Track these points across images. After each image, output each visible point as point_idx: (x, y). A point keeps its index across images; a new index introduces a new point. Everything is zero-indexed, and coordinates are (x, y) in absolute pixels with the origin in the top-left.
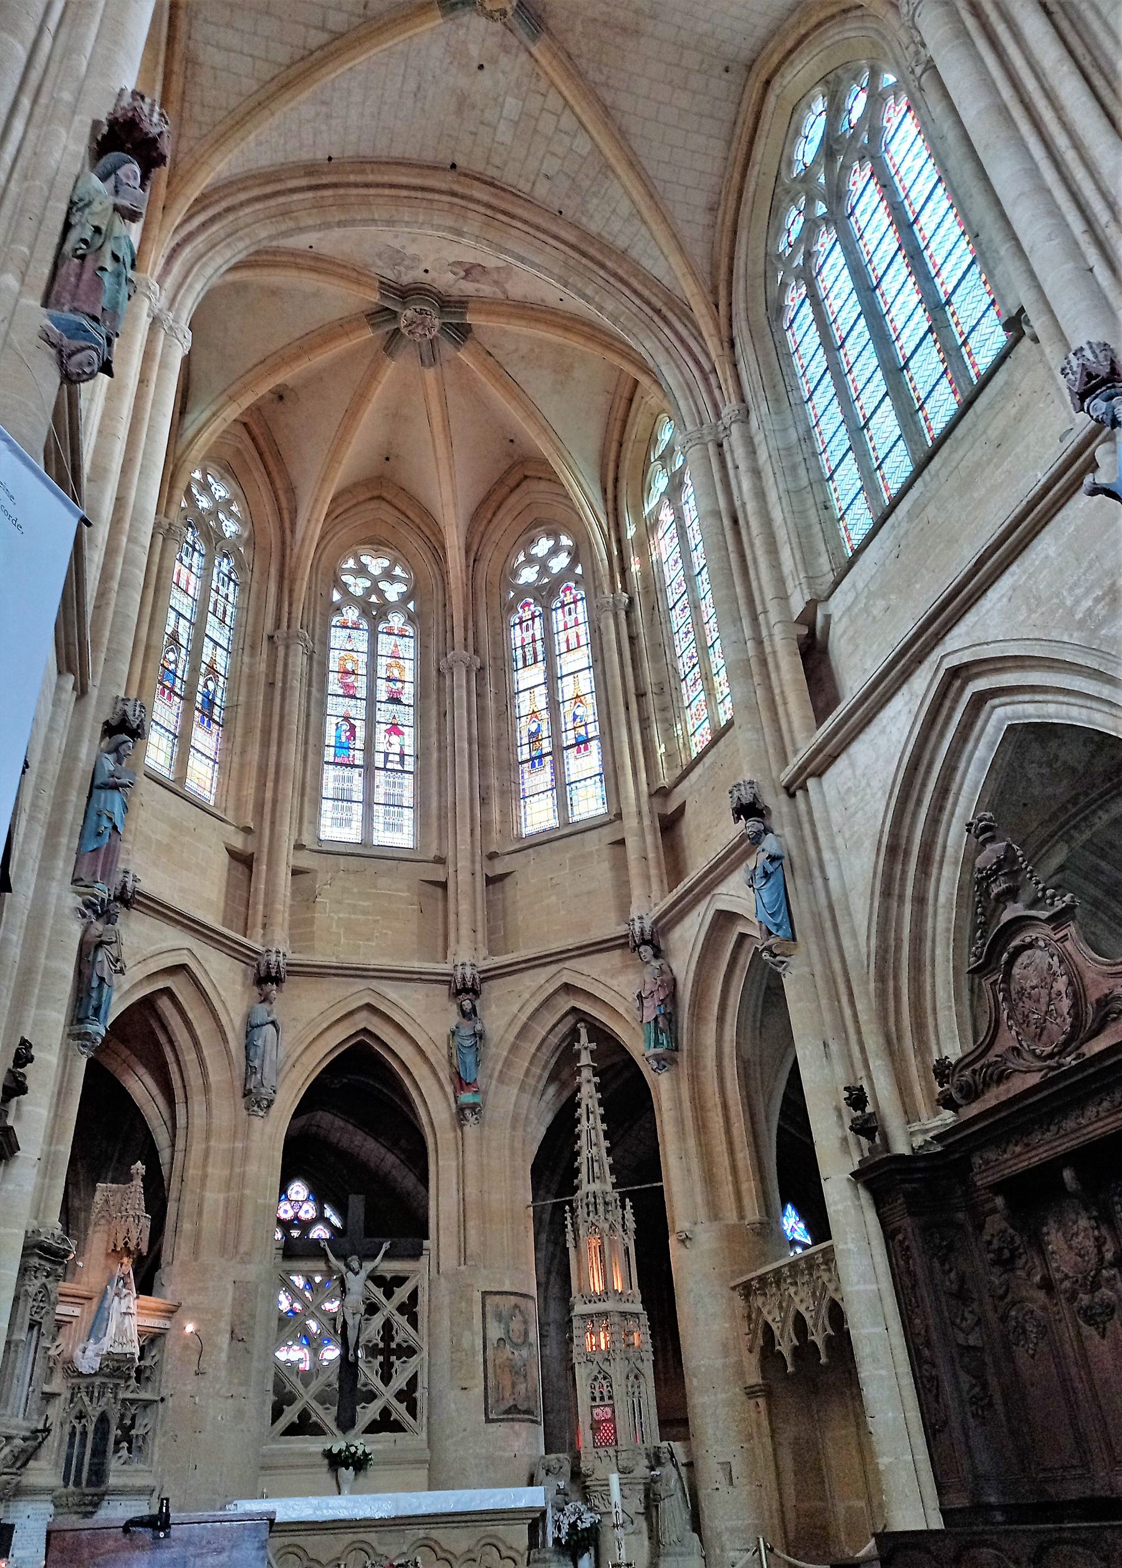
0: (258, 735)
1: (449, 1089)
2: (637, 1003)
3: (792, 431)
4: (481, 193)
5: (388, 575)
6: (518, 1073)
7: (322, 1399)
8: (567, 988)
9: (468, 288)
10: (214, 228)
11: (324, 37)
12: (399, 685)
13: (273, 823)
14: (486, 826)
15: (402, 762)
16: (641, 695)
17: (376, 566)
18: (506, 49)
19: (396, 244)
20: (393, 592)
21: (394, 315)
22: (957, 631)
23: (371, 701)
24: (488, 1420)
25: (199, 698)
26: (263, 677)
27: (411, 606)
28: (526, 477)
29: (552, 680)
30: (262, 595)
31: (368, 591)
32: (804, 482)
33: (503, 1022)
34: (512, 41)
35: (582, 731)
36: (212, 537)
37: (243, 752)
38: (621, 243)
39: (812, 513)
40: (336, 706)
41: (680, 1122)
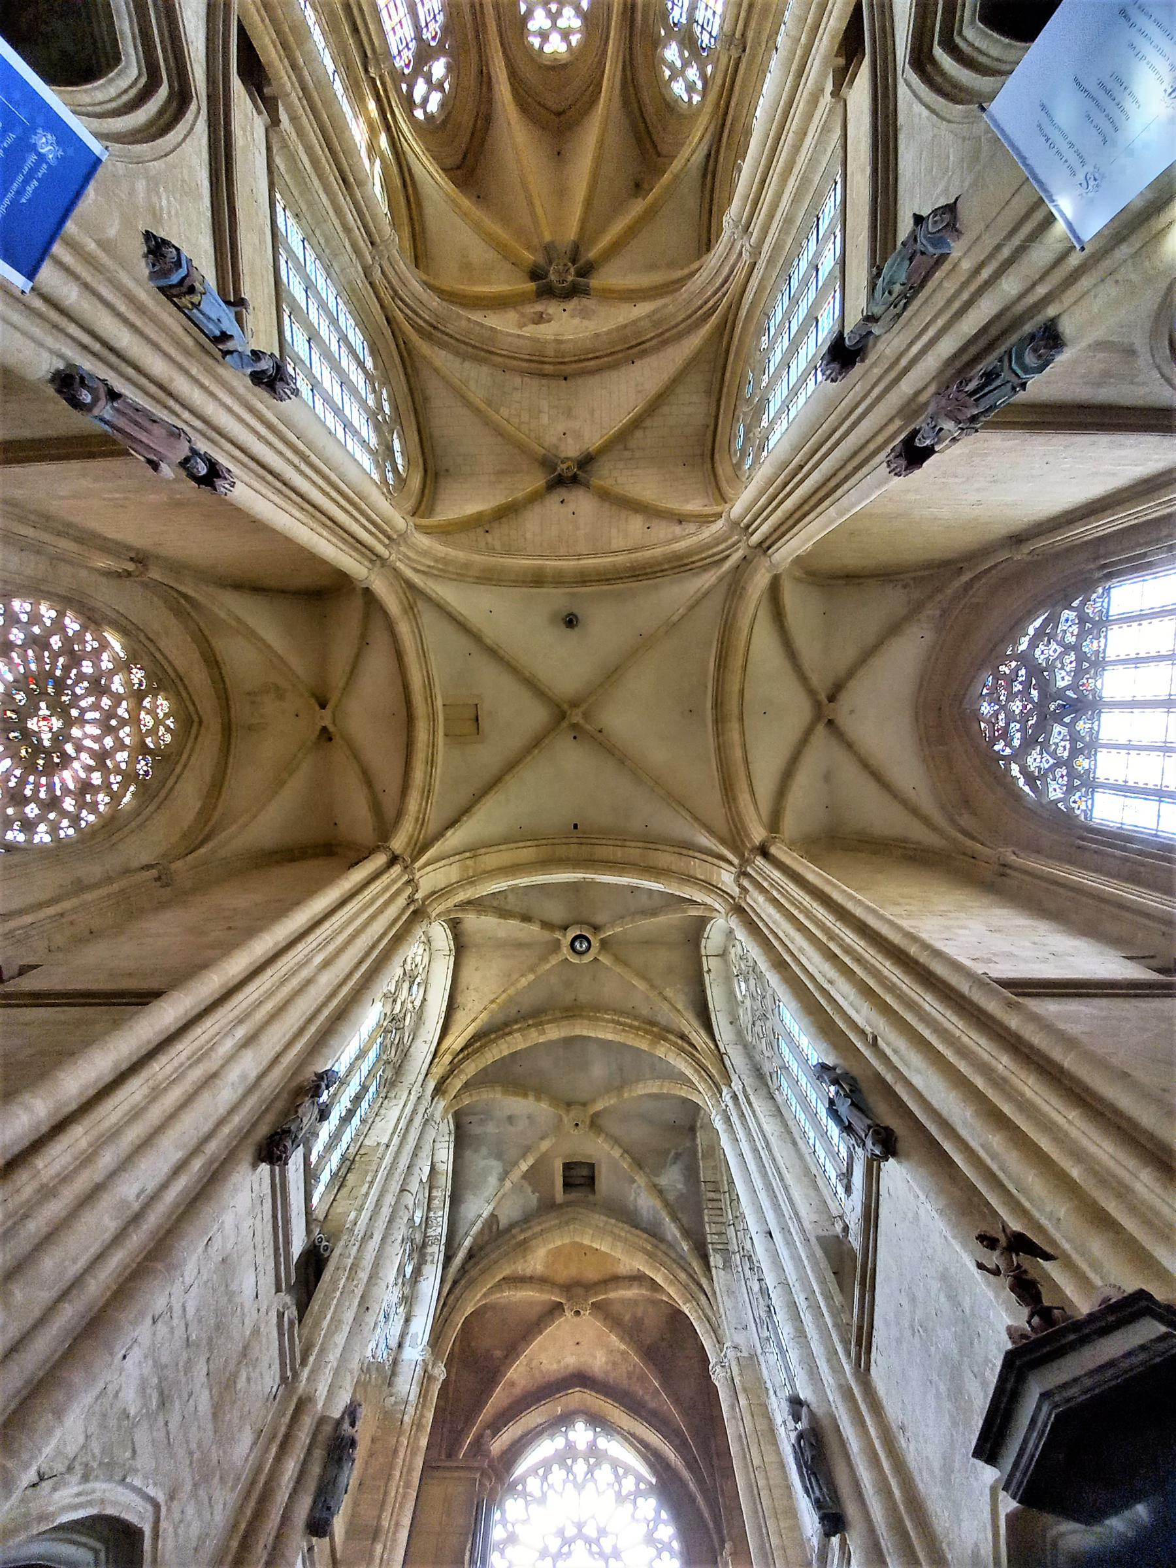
3: (338, 270)
10: (700, 303)
22: (205, 141)
32: (318, 232)
36: (688, 41)
39: (304, 208)
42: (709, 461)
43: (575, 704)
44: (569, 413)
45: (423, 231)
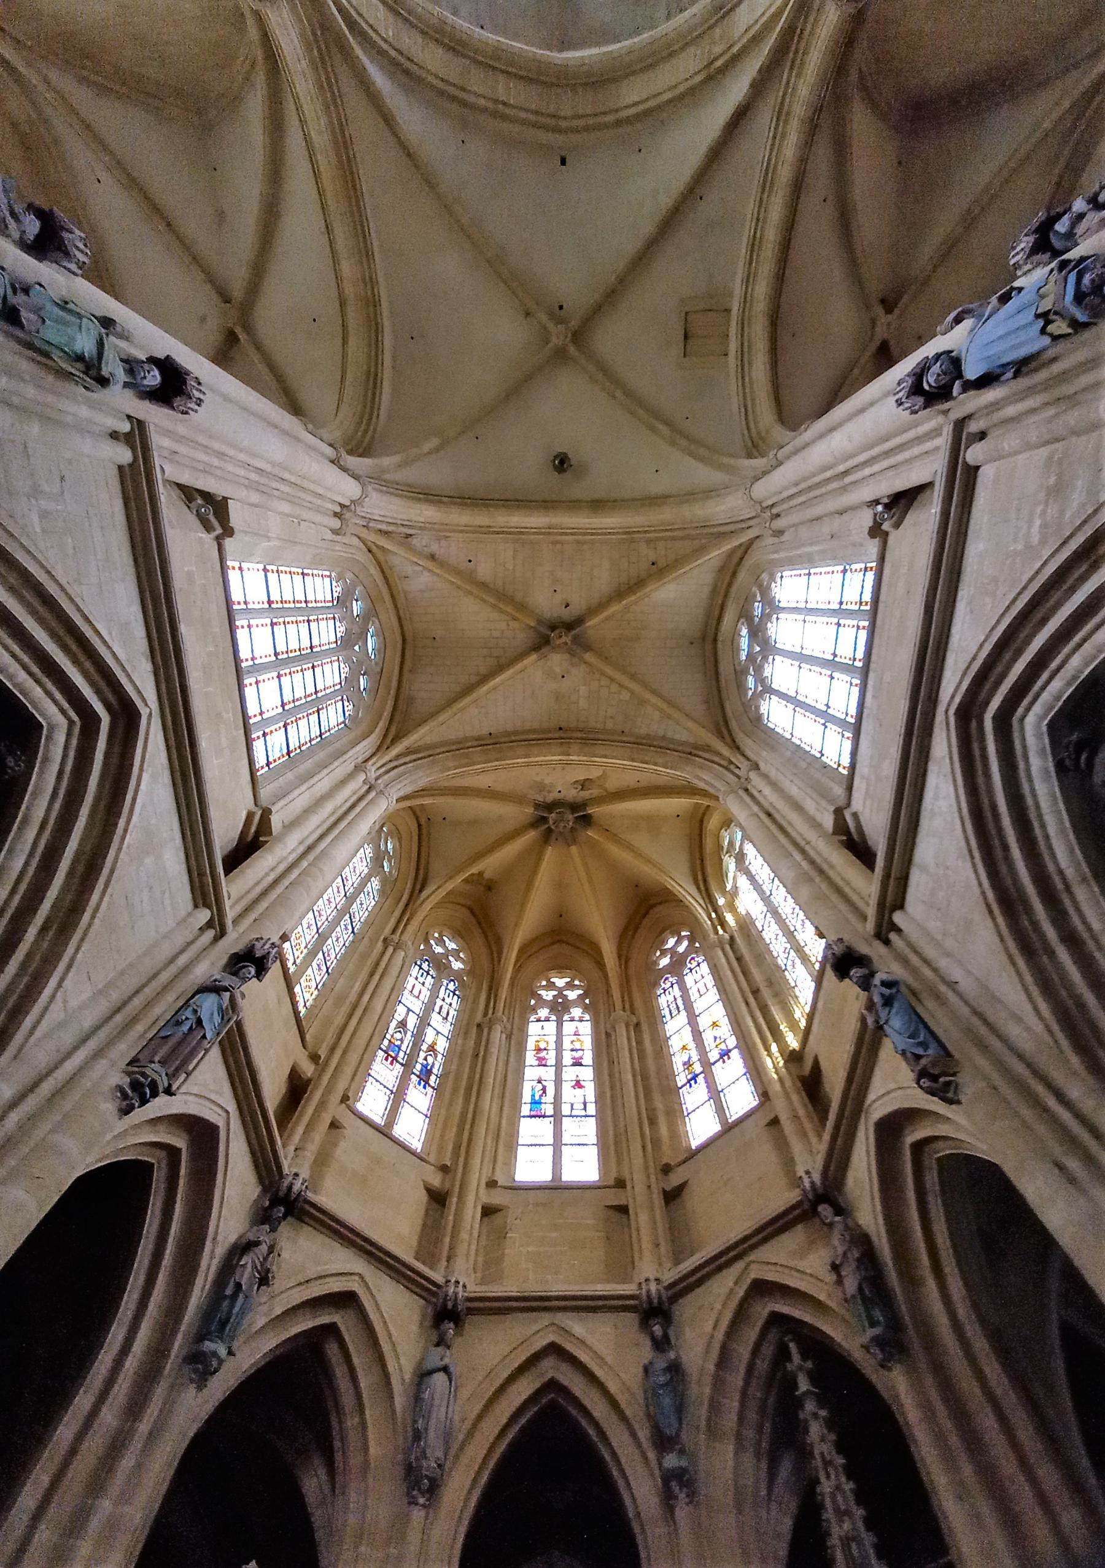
0: (462, 1091)
1: (652, 1455)
2: (834, 1277)
6: (729, 1420)
8: (761, 1288)
9: (586, 794)
11: (478, 678)
12: (580, 1053)
14: (656, 1142)
15: (585, 1109)
16: (756, 992)
17: (560, 982)
18: (573, 665)
19: (538, 779)
20: (572, 995)
21: (544, 820)
23: (559, 1066)
25: (419, 1067)
27: (587, 1001)
28: (652, 906)
29: (693, 1019)
33: (699, 1349)
34: (575, 660)
35: (723, 1046)
37: (451, 1104)
38: (661, 733)
40: (531, 1073)
41: (940, 1438)
42: (409, 637)
43: (560, 356)
44: (558, 697)
45: (692, 855)
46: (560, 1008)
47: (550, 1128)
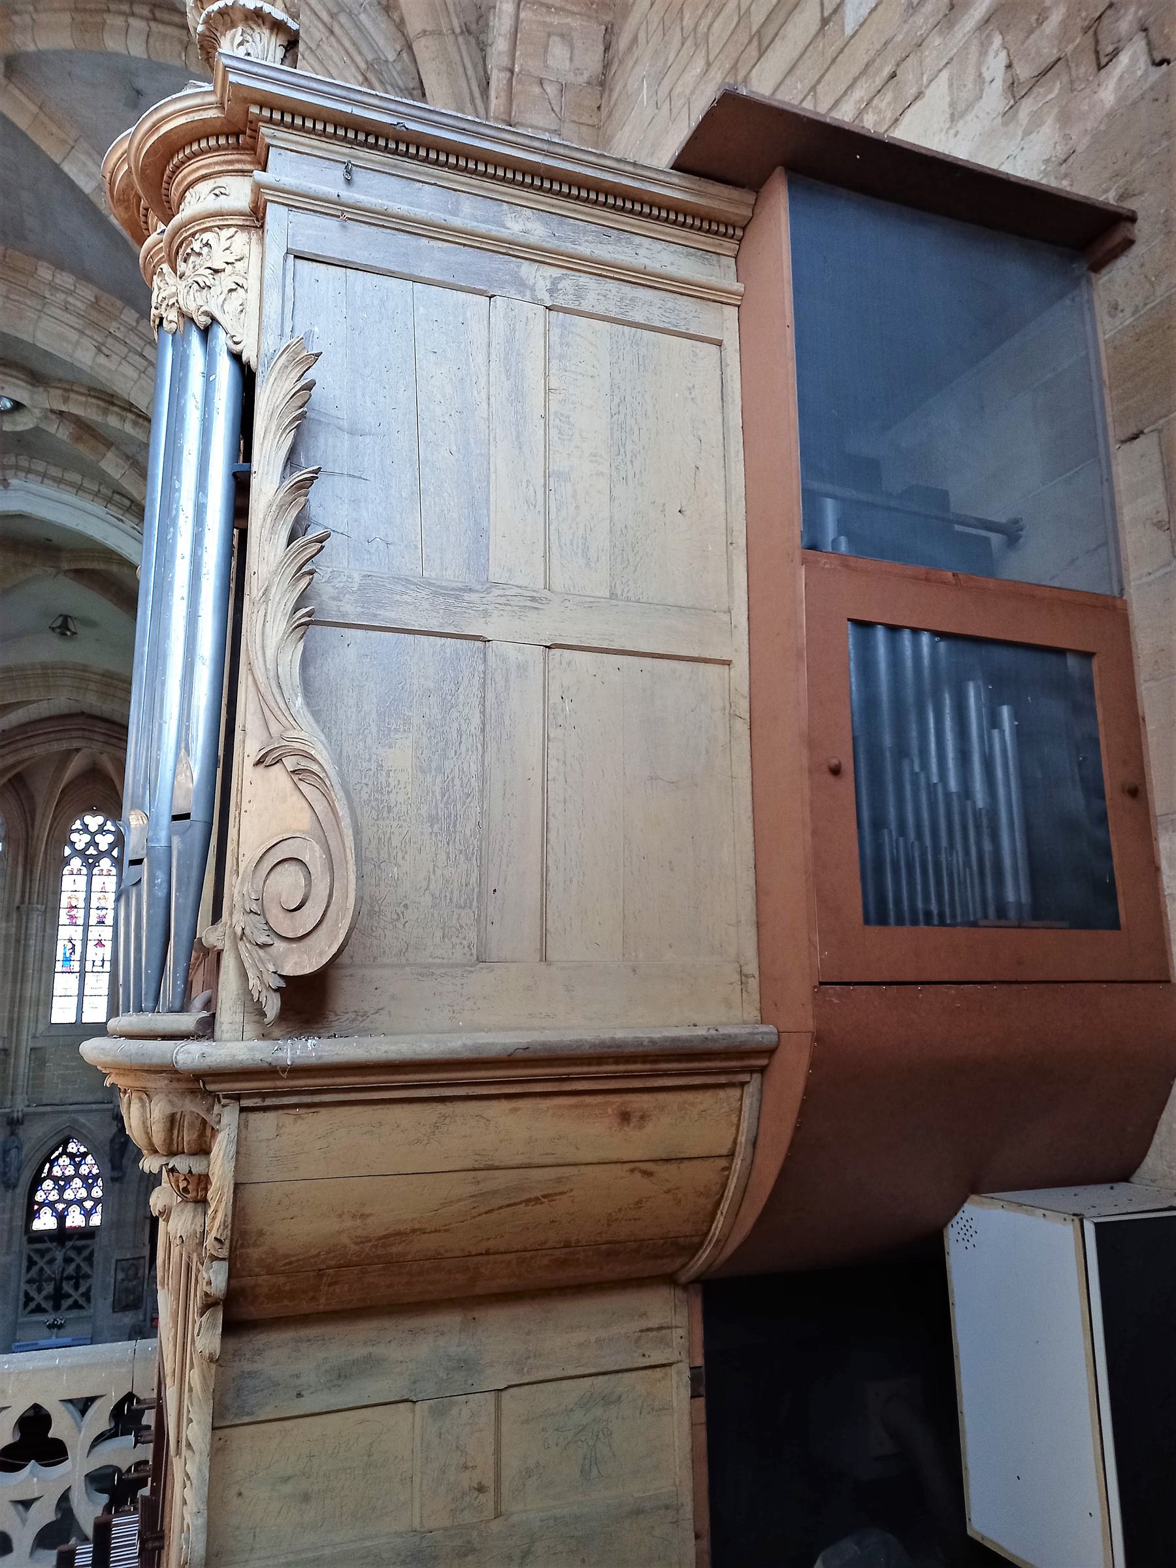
4: (101, 727)
5: (101, 830)
7: (46, 1298)
12: (104, 911)
13: (18, 1032)
15: (103, 966)
17: (93, 822)
20: (104, 841)
23: (86, 926)
24: (114, 1312)
26: (14, 937)
30: (14, 876)
31: (88, 845)
40: (64, 933)
46: (90, 863)
47: (77, 982)
